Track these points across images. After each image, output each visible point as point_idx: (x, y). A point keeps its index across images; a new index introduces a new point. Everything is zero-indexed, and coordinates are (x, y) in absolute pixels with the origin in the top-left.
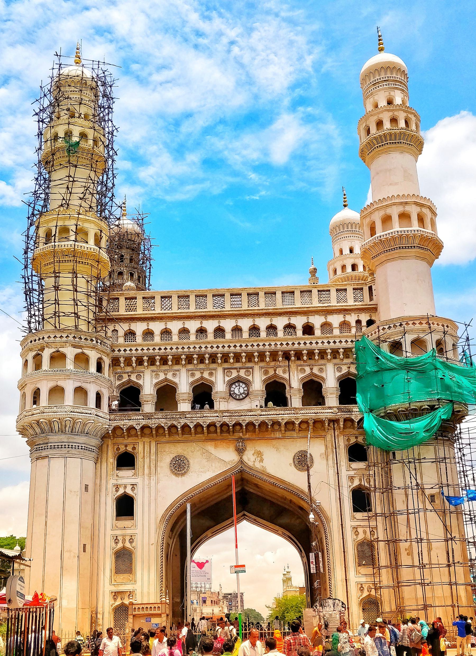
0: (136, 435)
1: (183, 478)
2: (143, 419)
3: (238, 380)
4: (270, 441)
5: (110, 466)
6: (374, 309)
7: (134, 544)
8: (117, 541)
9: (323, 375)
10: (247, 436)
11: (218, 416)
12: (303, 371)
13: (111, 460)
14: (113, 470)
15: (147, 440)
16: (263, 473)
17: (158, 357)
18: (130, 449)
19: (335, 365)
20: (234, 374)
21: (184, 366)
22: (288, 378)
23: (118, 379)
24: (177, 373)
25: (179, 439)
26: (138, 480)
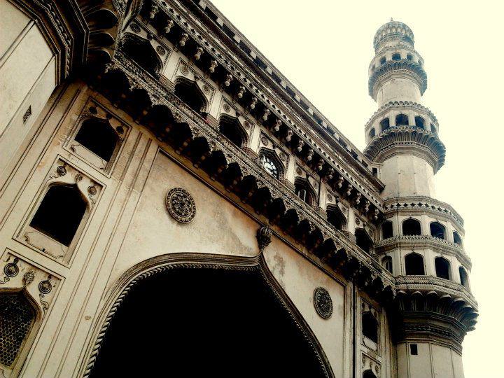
1: (180, 228)
2: (166, 97)
3: (270, 155)
4: (295, 252)
5: (67, 124)
6: (380, 188)
7: (47, 297)
8: (12, 268)
10: (274, 228)
11: (261, 174)
15: (147, 135)
18: (114, 124)
19: (356, 215)
20: (270, 146)
22: (317, 193)
25: (194, 170)
26: (109, 183)
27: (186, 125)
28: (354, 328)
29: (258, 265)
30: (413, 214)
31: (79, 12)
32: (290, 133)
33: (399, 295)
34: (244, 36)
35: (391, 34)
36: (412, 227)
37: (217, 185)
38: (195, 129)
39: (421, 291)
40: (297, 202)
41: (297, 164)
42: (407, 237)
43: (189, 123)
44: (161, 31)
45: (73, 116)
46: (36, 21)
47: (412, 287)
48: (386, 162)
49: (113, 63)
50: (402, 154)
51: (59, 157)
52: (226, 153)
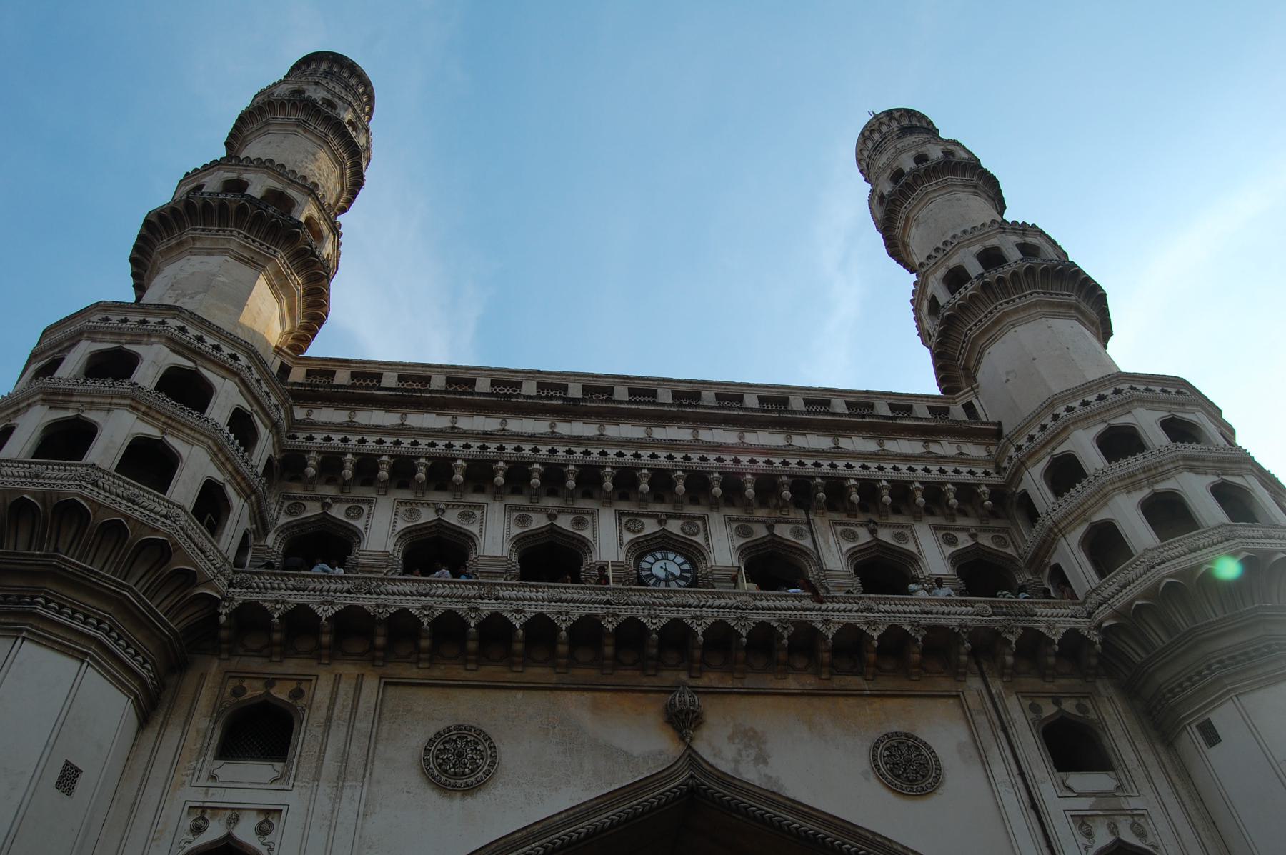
0: (317, 654)
1: (469, 801)
2: (349, 592)
3: (663, 543)
4: (783, 700)
6: (994, 433)
9: (910, 547)
10: (704, 682)
12: (852, 536)
13: (199, 721)
14: (202, 753)
15: (349, 670)
16: (774, 799)
17: (423, 460)
19: (936, 529)
20: (651, 527)
21: (498, 493)
22: (812, 547)
23: (289, 513)
24: (477, 513)
26: (292, 800)
27: (404, 612)
28: (1022, 774)
29: (692, 777)
30: (1053, 444)
31: (96, 573)
32: (678, 478)
33: (1105, 632)
34: (539, 372)
36: (1065, 473)
37: (536, 673)
38: (424, 608)
39: (1143, 596)
40: (723, 602)
41: (732, 520)
42: (1061, 500)
43: (404, 604)
44: (344, 485)
45: (201, 721)
46: (24, 634)
47: (1119, 602)
48: (979, 377)
49: (232, 600)
50: (993, 340)
51: (188, 804)
52: (505, 609)
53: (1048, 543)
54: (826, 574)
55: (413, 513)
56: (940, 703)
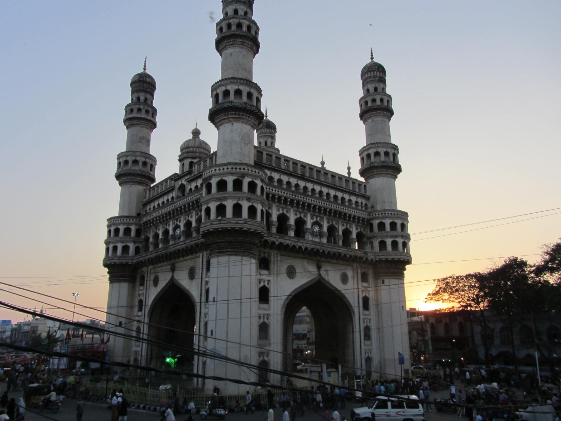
6: (368, 198)
9: (351, 230)
12: (343, 225)
15: (275, 252)
18: (266, 255)
20: (315, 220)
26: (271, 278)
27: (288, 244)
33: (376, 261)
35: (370, 77)
36: (382, 226)
47: (381, 257)
50: (378, 177)
52: (301, 245)
53: (373, 237)
54: (339, 235)
55: (278, 210)
56: (350, 268)
